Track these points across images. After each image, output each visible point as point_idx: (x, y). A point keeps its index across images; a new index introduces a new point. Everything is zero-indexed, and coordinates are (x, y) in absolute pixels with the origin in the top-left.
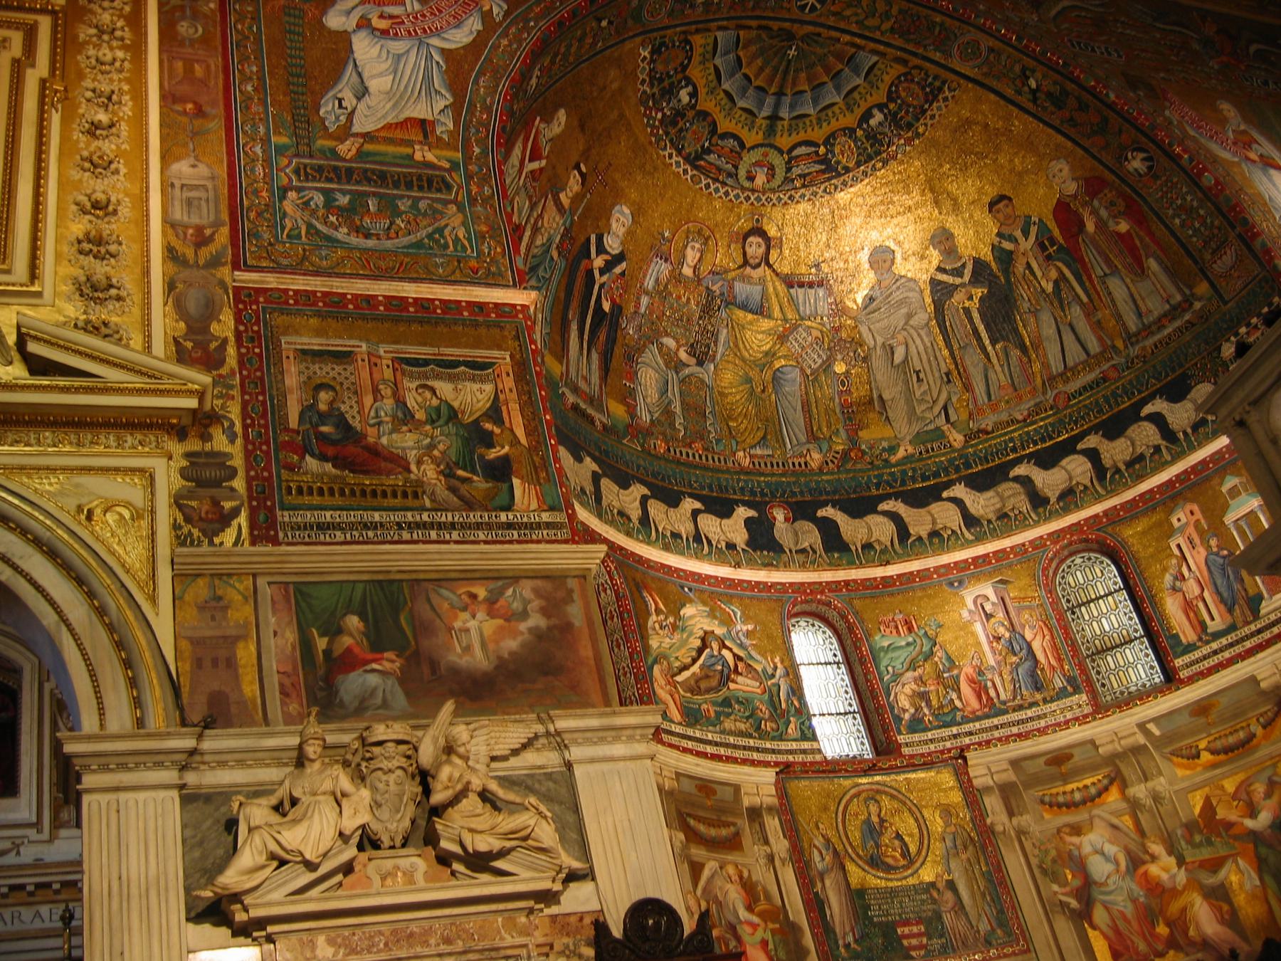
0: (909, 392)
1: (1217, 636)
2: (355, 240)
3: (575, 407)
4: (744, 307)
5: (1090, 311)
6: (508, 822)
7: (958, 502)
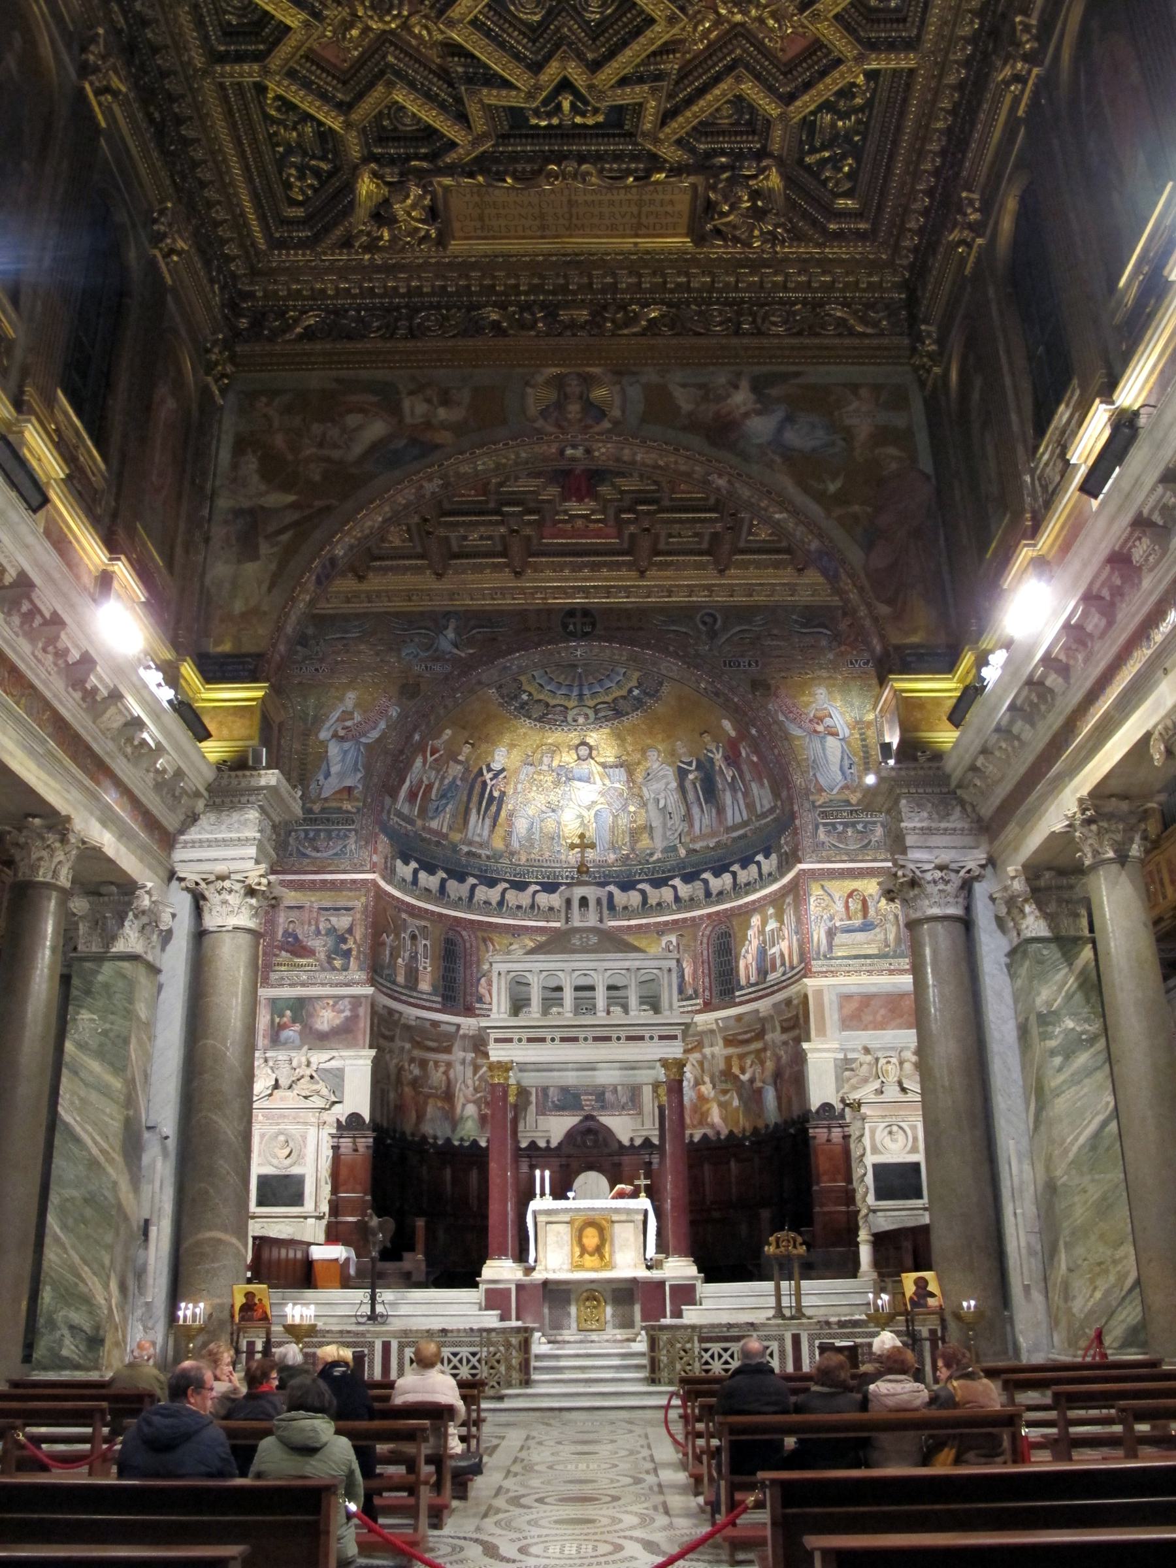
0: (664, 824)
1: (753, 985)
2: (314, 854)
3: (469, 853)
4: (580, 780)
5: (746, 794)
6: (315, 1087)
7: (674, 887)
